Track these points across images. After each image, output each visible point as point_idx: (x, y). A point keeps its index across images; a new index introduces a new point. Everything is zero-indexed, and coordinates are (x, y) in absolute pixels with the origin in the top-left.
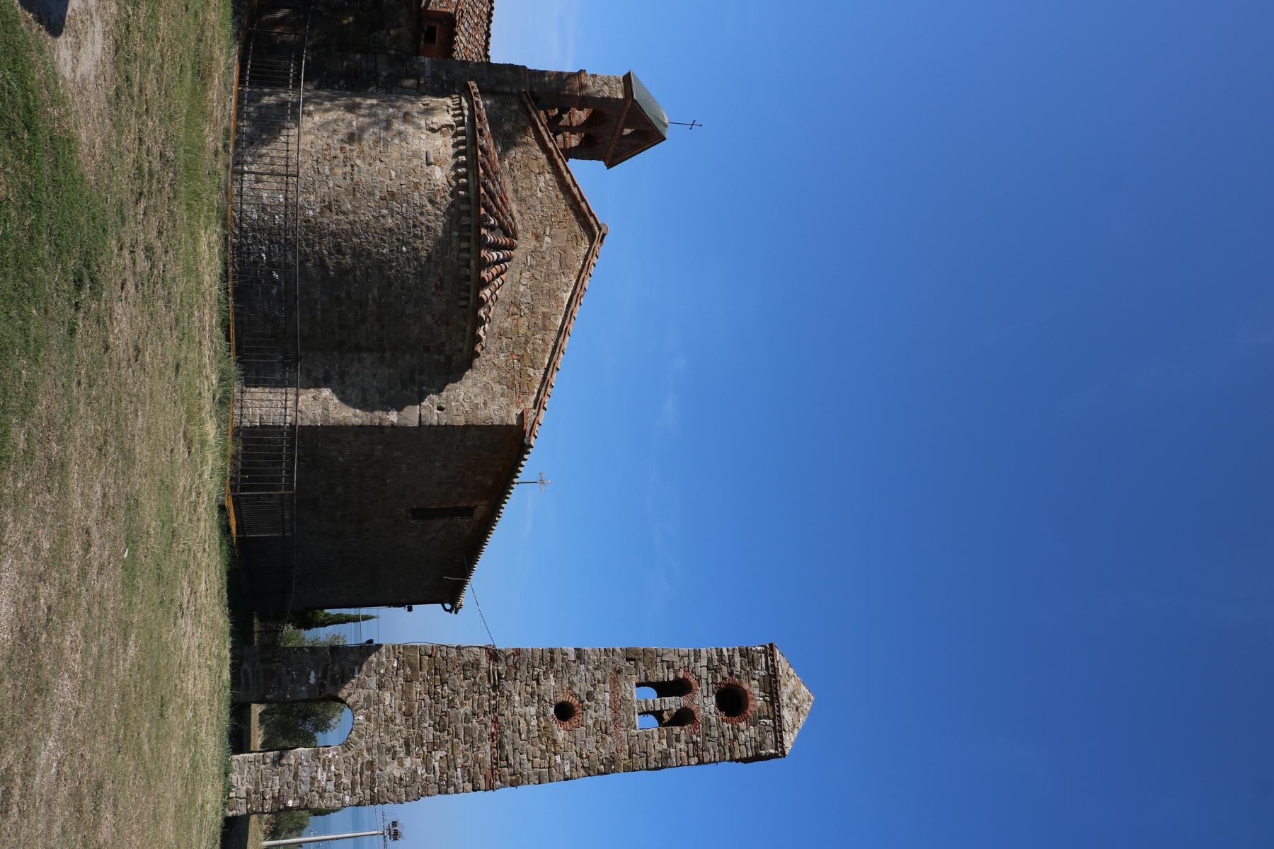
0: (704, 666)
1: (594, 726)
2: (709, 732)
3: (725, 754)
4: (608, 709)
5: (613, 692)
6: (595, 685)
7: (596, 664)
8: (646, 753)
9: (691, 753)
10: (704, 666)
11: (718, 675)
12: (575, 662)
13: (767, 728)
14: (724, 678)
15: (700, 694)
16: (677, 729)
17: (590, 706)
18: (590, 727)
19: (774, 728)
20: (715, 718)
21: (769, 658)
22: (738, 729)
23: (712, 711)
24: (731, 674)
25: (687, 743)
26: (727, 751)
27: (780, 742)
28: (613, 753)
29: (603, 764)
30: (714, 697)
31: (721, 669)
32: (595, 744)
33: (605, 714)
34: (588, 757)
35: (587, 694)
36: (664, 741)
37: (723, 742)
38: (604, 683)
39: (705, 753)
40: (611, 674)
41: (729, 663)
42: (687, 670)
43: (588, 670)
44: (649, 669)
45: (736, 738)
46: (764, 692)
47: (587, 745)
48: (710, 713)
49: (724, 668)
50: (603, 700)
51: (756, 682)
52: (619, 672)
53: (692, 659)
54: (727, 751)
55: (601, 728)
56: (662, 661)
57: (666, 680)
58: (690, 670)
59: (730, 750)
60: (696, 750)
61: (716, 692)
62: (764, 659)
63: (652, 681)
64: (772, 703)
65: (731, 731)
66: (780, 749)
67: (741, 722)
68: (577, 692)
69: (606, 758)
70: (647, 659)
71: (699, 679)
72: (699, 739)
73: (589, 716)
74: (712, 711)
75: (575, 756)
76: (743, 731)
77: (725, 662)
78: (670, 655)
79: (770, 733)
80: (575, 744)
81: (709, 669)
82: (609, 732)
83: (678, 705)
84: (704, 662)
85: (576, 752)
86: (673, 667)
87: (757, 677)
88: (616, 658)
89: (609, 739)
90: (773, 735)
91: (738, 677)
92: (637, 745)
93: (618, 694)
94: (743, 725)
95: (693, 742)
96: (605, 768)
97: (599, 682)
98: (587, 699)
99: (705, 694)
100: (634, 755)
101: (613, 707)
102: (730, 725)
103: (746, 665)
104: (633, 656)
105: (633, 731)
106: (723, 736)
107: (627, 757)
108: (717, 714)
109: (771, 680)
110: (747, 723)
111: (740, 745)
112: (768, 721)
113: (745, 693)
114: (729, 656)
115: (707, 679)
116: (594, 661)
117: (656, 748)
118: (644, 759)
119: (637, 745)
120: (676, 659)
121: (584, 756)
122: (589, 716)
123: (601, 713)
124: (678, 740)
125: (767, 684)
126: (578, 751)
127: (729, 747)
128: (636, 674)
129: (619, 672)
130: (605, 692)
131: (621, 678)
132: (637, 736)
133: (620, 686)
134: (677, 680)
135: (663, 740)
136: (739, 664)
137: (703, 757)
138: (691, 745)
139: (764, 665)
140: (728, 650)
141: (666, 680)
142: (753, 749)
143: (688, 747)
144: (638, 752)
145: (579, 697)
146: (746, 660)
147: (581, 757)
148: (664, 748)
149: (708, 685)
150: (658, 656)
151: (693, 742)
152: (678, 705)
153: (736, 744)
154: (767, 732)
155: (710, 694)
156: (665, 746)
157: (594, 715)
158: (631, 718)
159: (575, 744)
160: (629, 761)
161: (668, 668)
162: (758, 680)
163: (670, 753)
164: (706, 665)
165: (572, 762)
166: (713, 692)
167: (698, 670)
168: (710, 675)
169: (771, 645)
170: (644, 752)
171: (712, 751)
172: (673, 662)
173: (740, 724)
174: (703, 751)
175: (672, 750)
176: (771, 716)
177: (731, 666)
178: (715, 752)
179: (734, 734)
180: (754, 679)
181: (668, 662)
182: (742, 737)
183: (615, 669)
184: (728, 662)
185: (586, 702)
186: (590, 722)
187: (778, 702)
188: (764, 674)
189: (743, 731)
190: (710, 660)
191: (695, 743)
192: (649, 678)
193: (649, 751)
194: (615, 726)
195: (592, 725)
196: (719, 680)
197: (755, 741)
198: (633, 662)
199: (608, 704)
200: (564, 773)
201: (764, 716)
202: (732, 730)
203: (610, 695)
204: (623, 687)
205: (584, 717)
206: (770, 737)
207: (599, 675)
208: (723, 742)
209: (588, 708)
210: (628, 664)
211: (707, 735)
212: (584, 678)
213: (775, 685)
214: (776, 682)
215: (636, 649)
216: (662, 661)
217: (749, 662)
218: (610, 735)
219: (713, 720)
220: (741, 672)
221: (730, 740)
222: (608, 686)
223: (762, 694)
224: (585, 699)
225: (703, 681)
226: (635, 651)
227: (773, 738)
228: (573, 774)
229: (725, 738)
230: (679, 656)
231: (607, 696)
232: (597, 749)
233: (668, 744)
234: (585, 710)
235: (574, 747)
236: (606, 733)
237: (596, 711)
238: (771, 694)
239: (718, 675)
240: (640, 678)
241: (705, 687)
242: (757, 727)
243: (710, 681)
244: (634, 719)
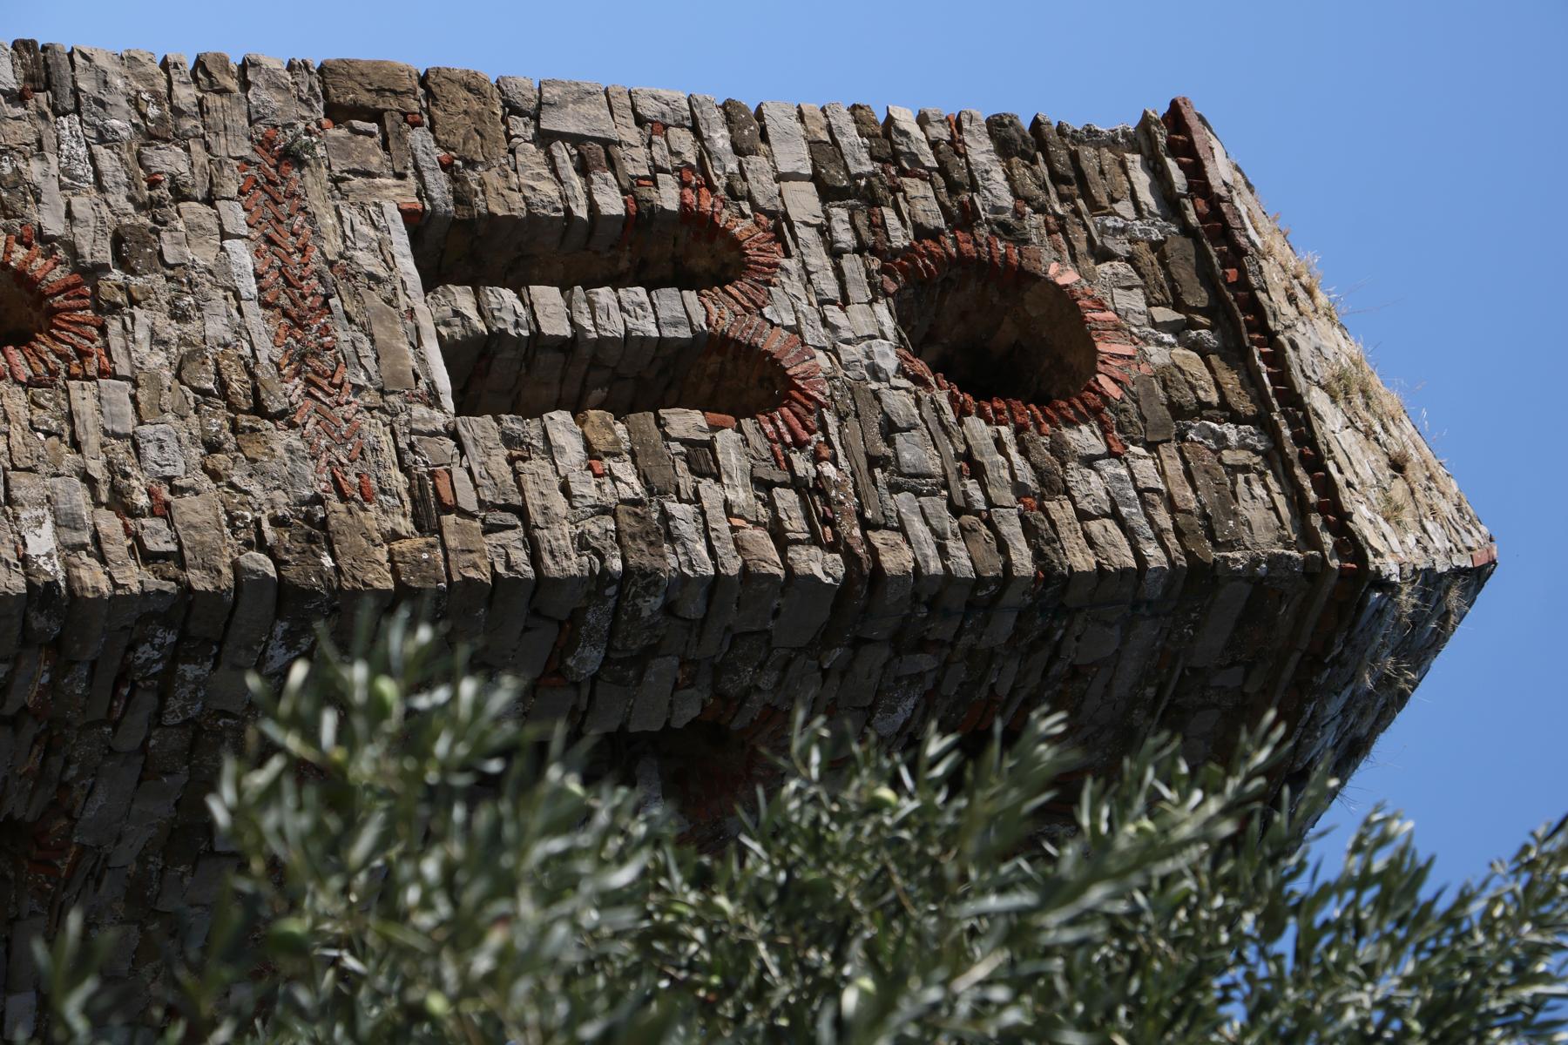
0: (795, 176)
1: (178, 376)
2: (882, 448)
3: (1003, 547)
4: (251, 308)
5: (270, 241)
6: (158, 203)
7: (153, 111)
8: (521, 512)
9: (796, 525)
10: (795, 176)
11: (889, 215)
12: (17, 98)
13: (1242, 457)
14: (921, 231)
15: (795, 286)
16: (686, 422)
17: (147, 293)
18: (155, 378)
19: (1274, 457)
20: (910, 401)
21: (1171, 164)
22: (1059, 450)
23: (889, 363)
24: (964, 218)
25: (763, 486)
26: (1012, 529)
27: (1321, 509)
28: (318, 500)
29: (260, 544)
30: (882, 310)
31: (896, 189)
32: (196, 453)
33: (241, 331)
34: (163, 511)
35: (118, 240)
36: (624, 469)
37: (977, 495)
38: (210, 200)
39: (877, 538)
40: (248, 162)
41: (943, 170)
42: (697, 174)
43: (104, 137)
44: (471, 164)
45: (1052, 485)
46: (1178, 305)
47: (151, 452)
48: (875, 372)
49: (916, 188)
50: (220, 273)
51: (1122, 268)
52: (292, 157)
53: (720, 139)
54: (1012, 529)
55: (223, 385)
56: (545, 139)
57: (582, 212)
58: (720, 183)
59: (1029, 529)
60: (827, 521)
61: (892, 288)
62: (1142, 180)
63: (500, 212)
64: (1236, 355)
65: (1013, 451)
66: (1328, 539)
67: (1070, 424)
68: (54, 225)
69: (277, 522)
70: (458, 127)
71: (779, 225)
72: (828, 469)
73: (142, 334)
74: (889, 363)
75: (82, 495)
76: (1089, 461)
77: (914, 159)
78: (584, 108)
79: (1252, 476)
80: (76, 445)
81: (828, 193)
82: (275, 407)
83: (675, 324)
84: (794, 157)
85: (88, 479)
86: (612, 164)
87: (1120, 246)
88: (262, 95)
89: (281, 439)
90: (1275, 487)
91: (1006, 230)
92: (460, 474)
93: (303, 250)
94: (1085, 438)
95: (797, 484)
96: (278, 563)
97: (180, 194)
98: (121, 261)
99: (831, 289)
100: (449, 520)
101: (284, 301)
102: (1006, 432)
103: (1043, 187)
104: (366, 98)
105: (419, 410)
106: (977, 471)
107: (405, 525)
108: (918, 380)
109: (1203, 256)
110: (1106, 433)
111: (1083, 516)
112: (1231, 432)
113: (1063, 294)
114: (934, 145)
115: (824, 231)
116: (135, 102)
117: (576, 489)
118: (513, 537)
119: (460, 474)
120: (631, 134)
121: (143, 501)
122: (142, 334)
123: (217, 327)
124: (702, 458)
125: (1185, 274)
126: (97, 469)
127: (1023, 518)
128: (401, 176)
129: (292, 157)
130: (224, 235)
131: (313, 185)
132: (454, 435)
133: (311, 218)
134: (642, 218)
135: (607, 461)
136: (998, 176)
137: (873, 551)
138: (787, 499)
139: (1146, 197)
140: (923, 120)
141: (582, 212)
142: (1172, 541)
143: (770, 504)
144: (468, 500)
145: (71, 248)
146: (1042, 169)
147: (120, 503)
148: (627, 493)
149: (835, 253)
150: (512, 109)
151: (797, 484)
152: (675, 324)
153: (1061, 511)
154: (1234, 469)
155: (859, 292)
156: (630, 484)
157: (171, 330)
158: (400, 355)
159: (76, 445)
160: (419, 542)
161: (583, 169)
162: (1131, 259)
163: (666, 517)
164: (808, 171)
165: (67, 521)
166: (877, 292)
167: (762, 187)
168: (840, 214)
169: (1175, 117)
170: (507, 508)
171: (918, 528)
172: (607, 143)
173: (1070, 435)
174: (866, 525)
175: (674, 508)
176: (1246, 406)
177: (953, 188)
178: (939, 537)
179: (1034, 466)
180: (1104, 255)
181: (576, 140)
182: (1091, 487)
183: (265, 144)
184: (930, 160)
185: (117, 275)
186: (157, 360)
187: (1271, 338)
188: (1156, 235)
189: (1089, 461)
190: (825, 150)
191: (811, 491)
192: (479, 200)
193: (534, 502)
194: (309, 382)
195: (167, 376)
196: (900, 237)
197: (1172, 508)
198: (374, 127)
199: (249, 287)
200: (24, 560)
201: (1204, 405)
202: (1024, 451)
203: (258, 253)
204: (330, 220)
205: (116, 342)
206: (1258, 490)
207: (169, 160)
208: (977, 495)
209: (133, 302)
210: (342, 132)
211: (874, 461)
212: (84, 170)
213: (1232, 275)
214: (1237, 254)
215: (377, 66)
216: (545, 139)
217: (1057, 178)
218: (284, 417)
219: (899, 402)
220: (1019, 214)
221: (1020, 490)
222: (235, 216)
223: (1164, 314)
224: (106, 256)
225: (804, 233)
226: (384, 82)
227: (1281, 502)
228: (84, 573)
229: (991, 474)
230: (640, 121)
231: (242, 256)
232: (215, 475)
233: (643, 476)
234: (115, 308)
235: (70, 459)
236: (259, 409)
237: (179, 315)
238: (1217, 312)
239: (889, 215)
240: (424, 192)
241: (818, 259)
242: (1168, 451)
243: (844, 237)
244: (422, 360)
